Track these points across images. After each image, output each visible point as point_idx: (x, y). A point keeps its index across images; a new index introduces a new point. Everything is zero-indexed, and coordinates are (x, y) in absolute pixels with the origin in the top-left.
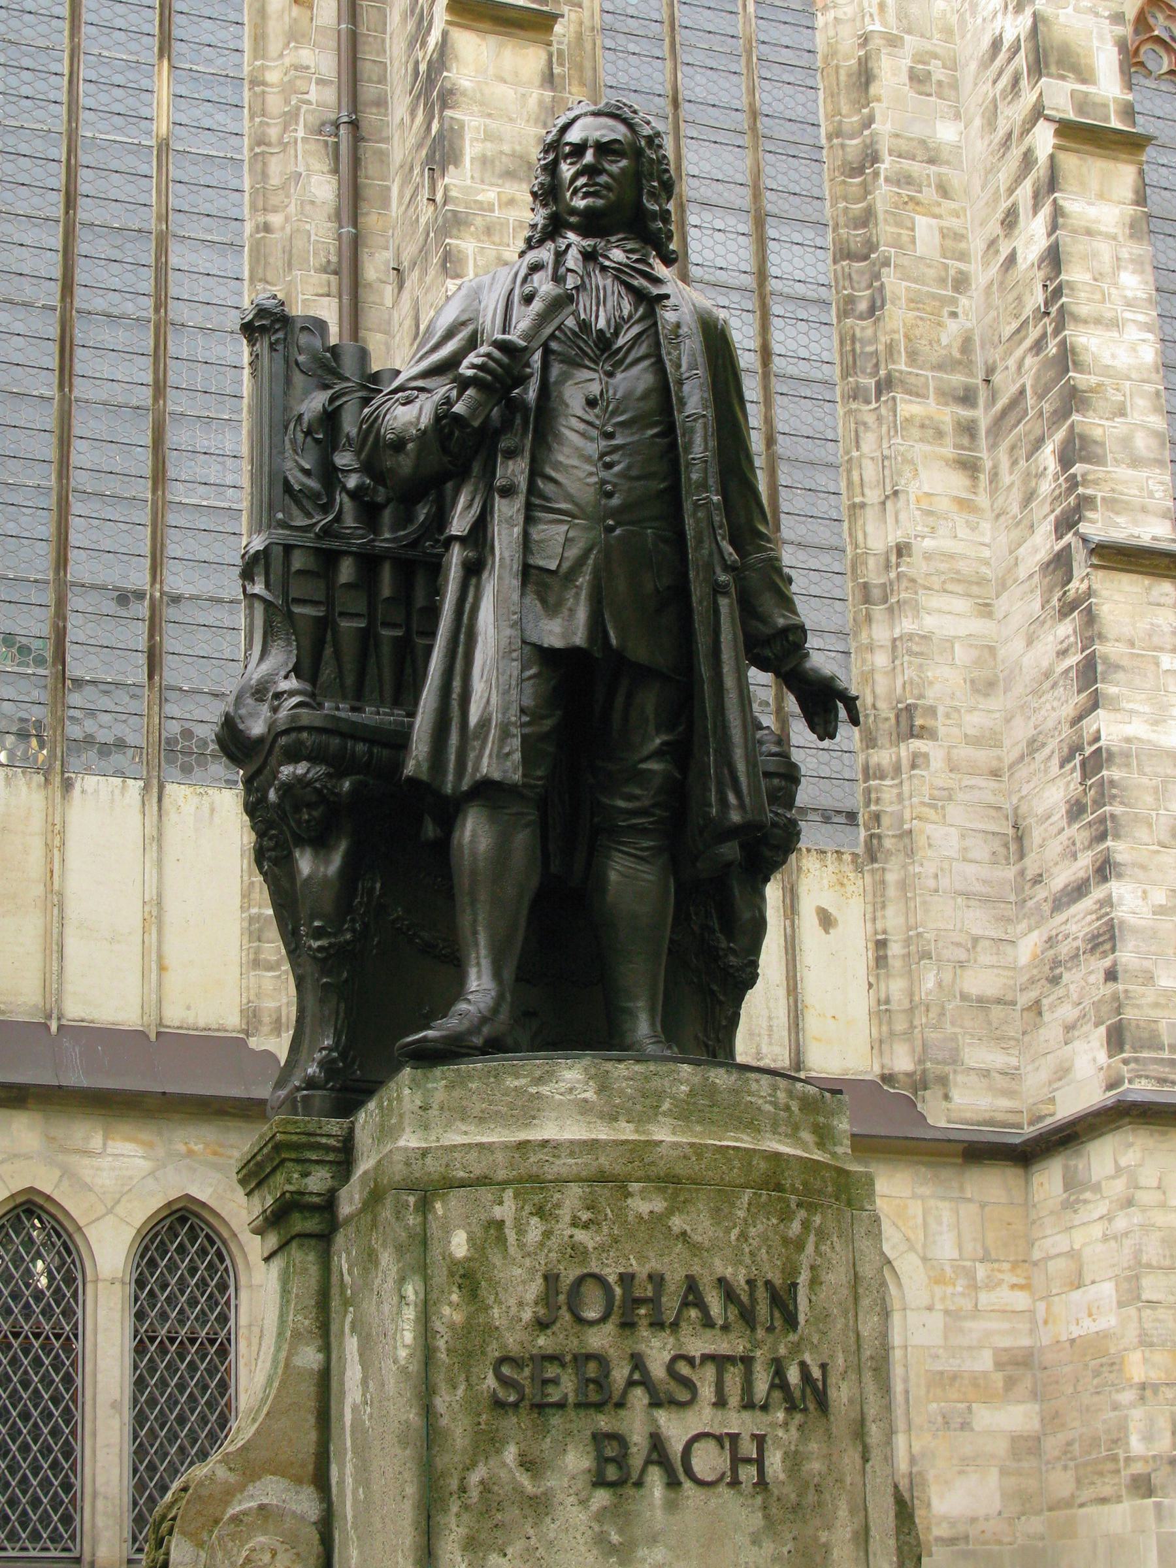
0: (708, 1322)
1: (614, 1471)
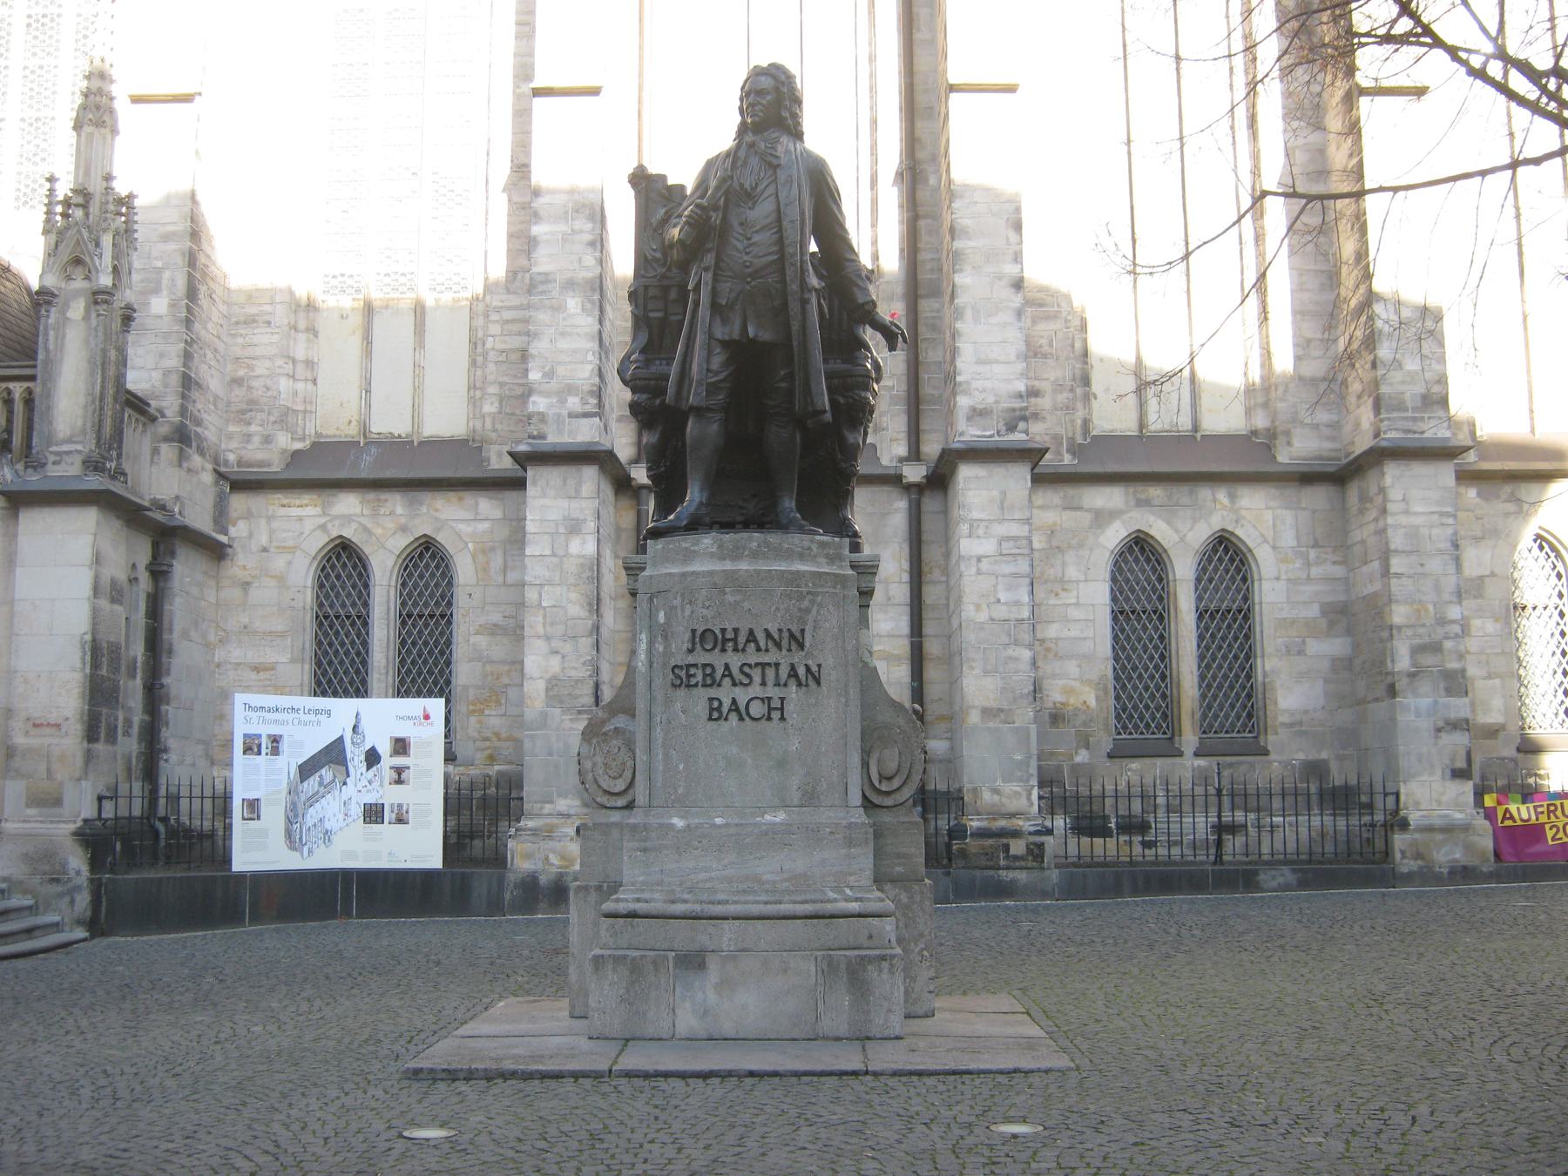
0: (759, 649)
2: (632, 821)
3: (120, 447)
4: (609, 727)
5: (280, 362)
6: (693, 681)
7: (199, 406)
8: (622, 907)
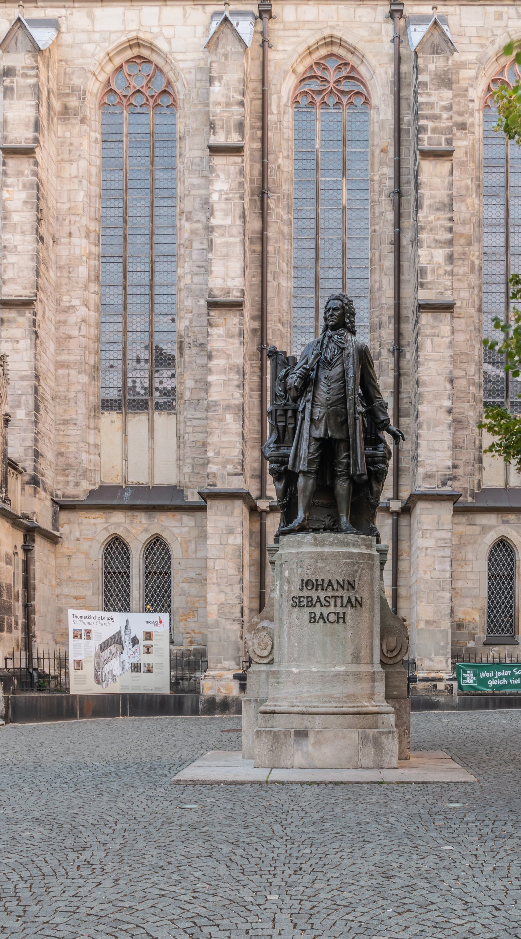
0: (333, 589)
1: (313, 619)
2: (273, 669)
3: (6, 486)
4: (259, 626)
5: (81, 445)
6: (302, 604)
7: (43, 466)
8: (268, 709)
